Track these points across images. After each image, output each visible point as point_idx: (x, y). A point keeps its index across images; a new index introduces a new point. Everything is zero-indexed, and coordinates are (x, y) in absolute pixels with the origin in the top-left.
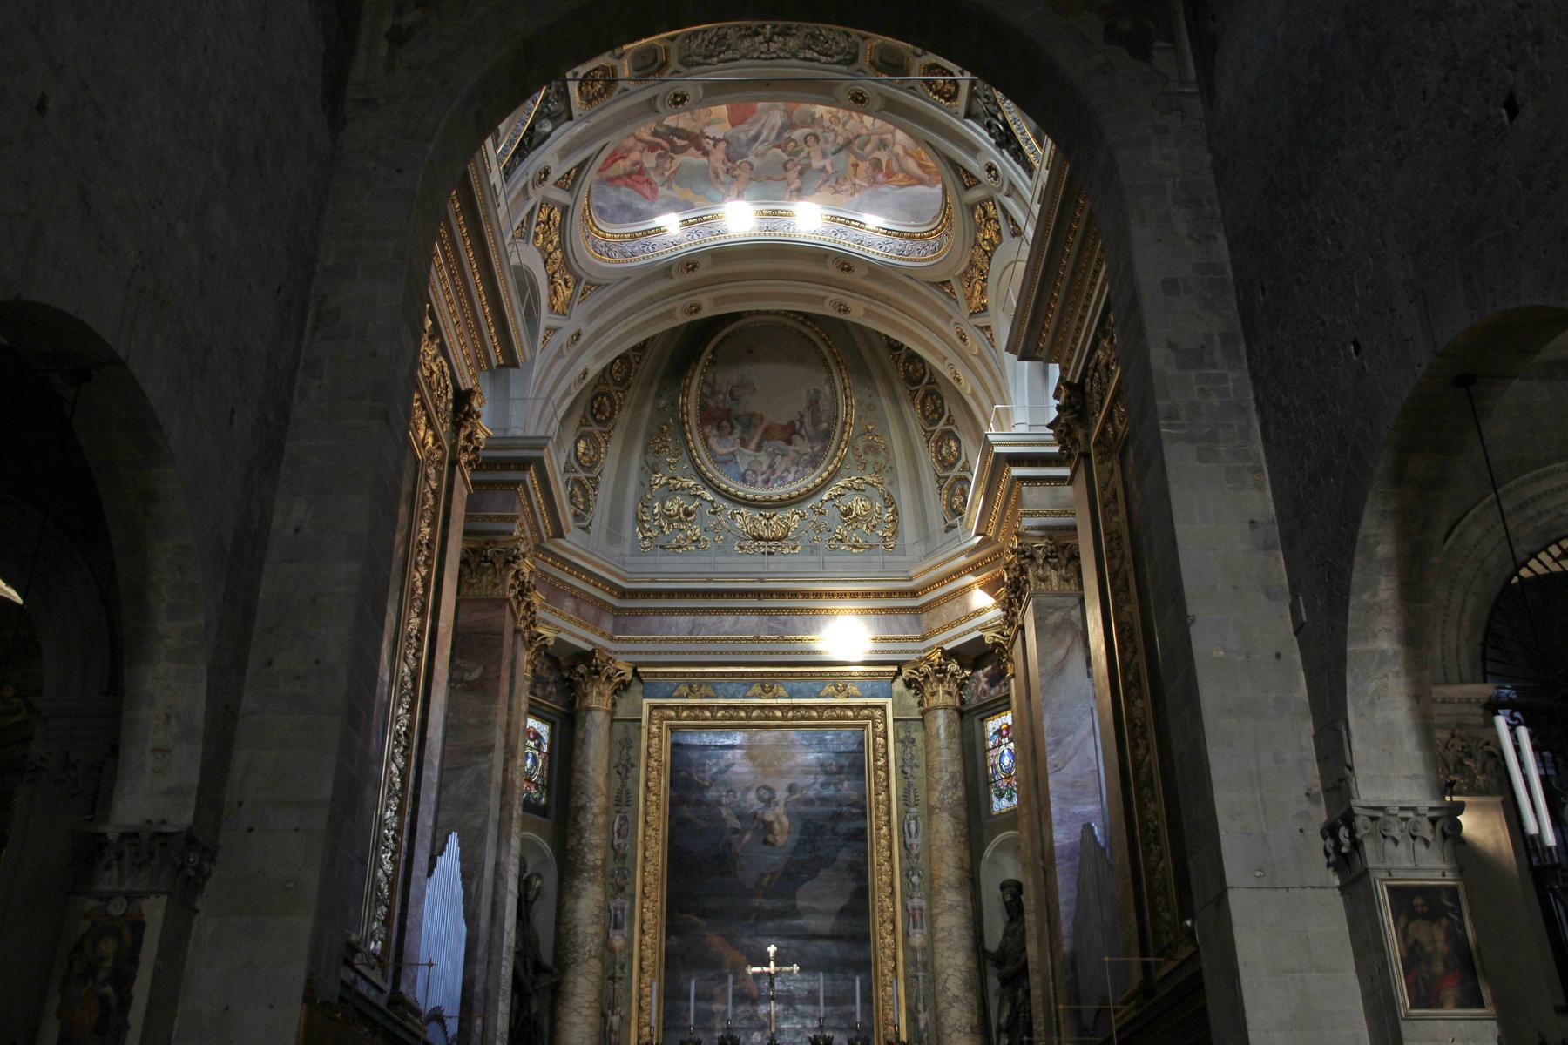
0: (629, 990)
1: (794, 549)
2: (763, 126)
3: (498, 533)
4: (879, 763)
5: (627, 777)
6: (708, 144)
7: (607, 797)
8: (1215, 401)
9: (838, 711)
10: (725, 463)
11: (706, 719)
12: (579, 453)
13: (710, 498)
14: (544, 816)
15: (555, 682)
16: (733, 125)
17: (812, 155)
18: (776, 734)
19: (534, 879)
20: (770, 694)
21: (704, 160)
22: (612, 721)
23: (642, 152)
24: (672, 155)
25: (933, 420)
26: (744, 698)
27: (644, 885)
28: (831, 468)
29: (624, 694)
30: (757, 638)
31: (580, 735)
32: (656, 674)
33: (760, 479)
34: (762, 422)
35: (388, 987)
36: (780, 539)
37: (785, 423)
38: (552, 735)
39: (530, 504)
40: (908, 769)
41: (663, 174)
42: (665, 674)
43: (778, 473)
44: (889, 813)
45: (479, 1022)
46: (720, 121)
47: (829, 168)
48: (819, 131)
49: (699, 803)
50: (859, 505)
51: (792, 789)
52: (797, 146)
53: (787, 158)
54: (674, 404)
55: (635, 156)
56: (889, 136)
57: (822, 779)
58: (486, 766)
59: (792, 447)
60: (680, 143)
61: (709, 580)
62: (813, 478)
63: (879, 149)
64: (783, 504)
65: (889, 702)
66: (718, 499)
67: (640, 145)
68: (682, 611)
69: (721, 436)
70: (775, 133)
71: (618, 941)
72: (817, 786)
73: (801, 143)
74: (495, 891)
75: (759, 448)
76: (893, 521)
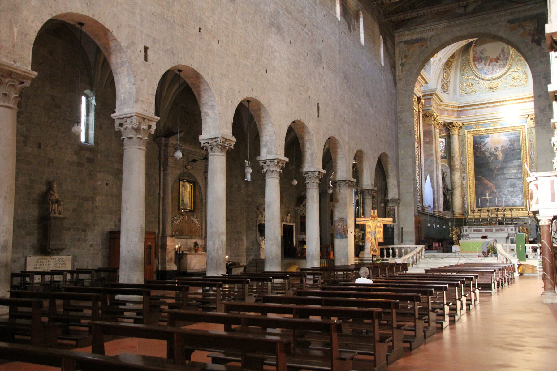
0: (468, 192)
1: (500, 89)
3: (428, 110)
5: (463, 148)
7: (459, 153)
8: (546, 118)
10: (480, 70)
11: (481, 133)
12: (444, 77)
13: (478, 80)
14: (446, 159)
15: (445, 130)
18: (498, 134)
19: (445, 173)
22: (459, 136)
27: (469, 171)
28: (508, 67)
29: (461, 129)
30: (492, 114)
31: (452, 140)
32: (468, 124)
33: (490, 73)
35: (421, 205)
36: (496, 88)
37: (495, 57)
38: (445, 141)
39: (435, 100)
42: (470, 124)
43: (494, 71)
44: (526, 150)
45: (437, 204)
49: (480, 151)
50: (516, 75)
51: (502, 147)
54: (466, 58)
57: (510, 143)
58: (432, 158)
59: (498, 63)
61: (478, 102)
62: (504, 70)
64: (496, 79)
66: (480, 80)
68: (472, 109)
69: (479, 63)
71: (464, 183)
72: (509, 146)
74: (437, 180)
75: (489, 65)
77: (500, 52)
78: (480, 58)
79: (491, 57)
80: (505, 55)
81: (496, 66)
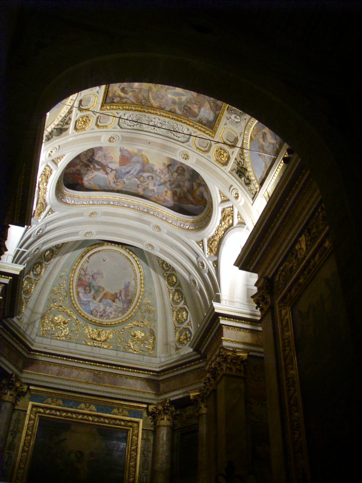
2: (132, 168)
4: (132, 448)
6: (109, 170)
9: (118, 422)
10: (85, 304)
16: (120, 165)
17: (150, 184)
20: (89, 409)
21: (106, 176)
23: (81, 166)
24: (93, 170)
25: (178, 302)
26: (76, 408)
33: (99, 314)
34: (103, 291)
37: (113, 293)
40: (145, 453)
41: (88, 177)
43: (107, 313)
46: (115, 163)
47: (155, 190)
48: (154, 176)
52: (144, 179)
53: (139, 183)
55: (78, 167)
56: (182, 183)
59: (114, 304)
60: (97, 167)
63: (177, 187)
65: (141, 421)
67: (81, 164)
70: (136, 172)
73: (146, 178)
75: (100, 301)
76: (153, 342)
77: (122, 287)
78: (90, 285)
79: (107, 289)
80: (128, 295)
81: (111, 306)
